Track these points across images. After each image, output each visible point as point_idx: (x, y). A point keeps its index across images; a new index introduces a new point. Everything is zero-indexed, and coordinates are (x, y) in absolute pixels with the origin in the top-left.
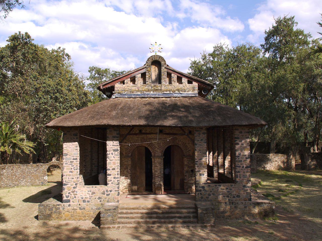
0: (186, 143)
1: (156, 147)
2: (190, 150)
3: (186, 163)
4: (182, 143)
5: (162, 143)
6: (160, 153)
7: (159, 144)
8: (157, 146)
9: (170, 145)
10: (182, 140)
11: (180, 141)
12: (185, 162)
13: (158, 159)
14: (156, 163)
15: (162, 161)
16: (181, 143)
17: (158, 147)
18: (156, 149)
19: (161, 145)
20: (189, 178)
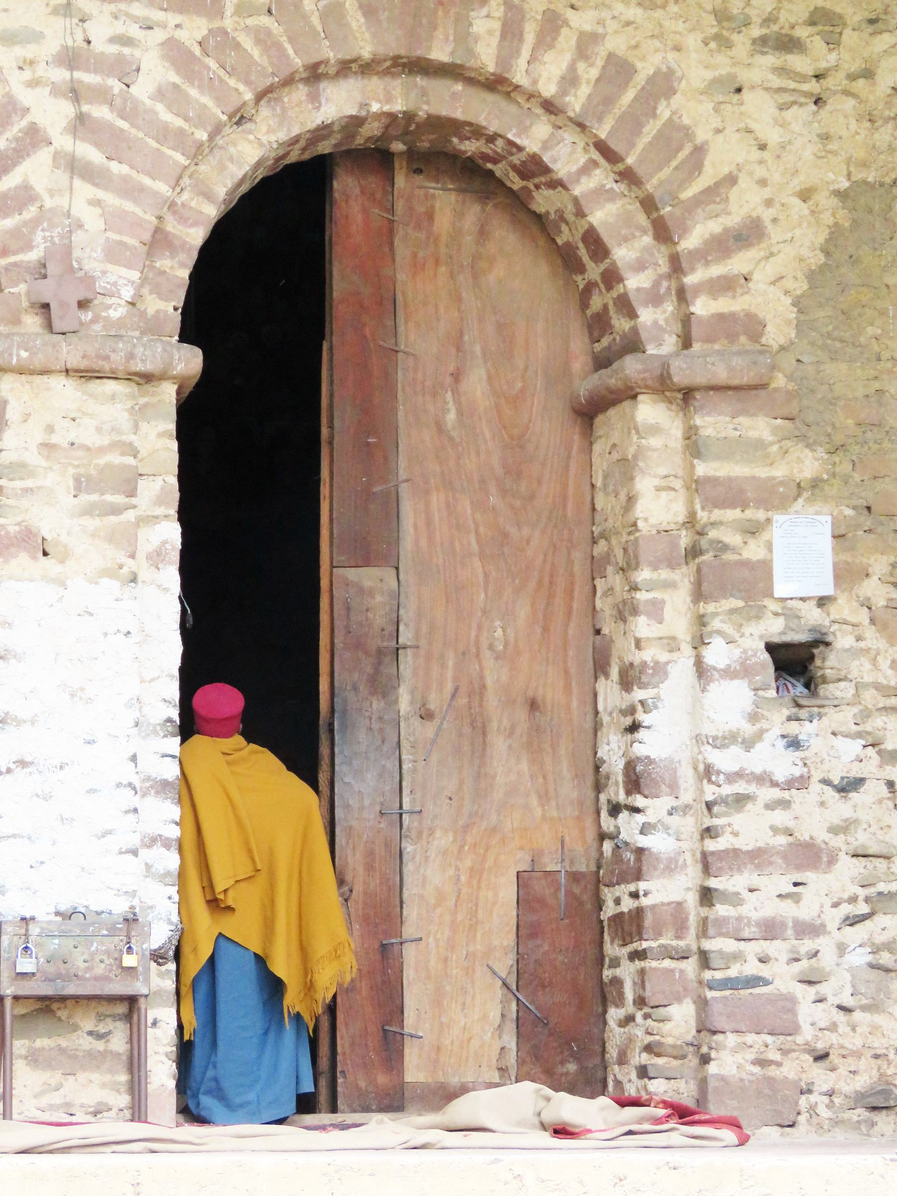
0: (663, 85)
1: (34, 137)
2: (749, 234)
3: (657, 507)
4: (589, 73)
5: (175, 53)
6: (115, 254)
7: (100, 65)
8: (52, 114)
9: (338, 102)
10: (582, 21)
11: (552, 25)
12: (644, 485)
13: (64, 392)
14: (19, 469)
15: (159, 446)
16: (570, 80)
17: (81, 124)
18: (36, 171)
19: (142, 90)
20: (741, 800)
